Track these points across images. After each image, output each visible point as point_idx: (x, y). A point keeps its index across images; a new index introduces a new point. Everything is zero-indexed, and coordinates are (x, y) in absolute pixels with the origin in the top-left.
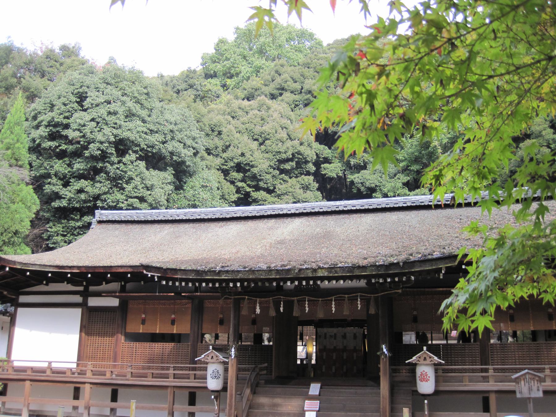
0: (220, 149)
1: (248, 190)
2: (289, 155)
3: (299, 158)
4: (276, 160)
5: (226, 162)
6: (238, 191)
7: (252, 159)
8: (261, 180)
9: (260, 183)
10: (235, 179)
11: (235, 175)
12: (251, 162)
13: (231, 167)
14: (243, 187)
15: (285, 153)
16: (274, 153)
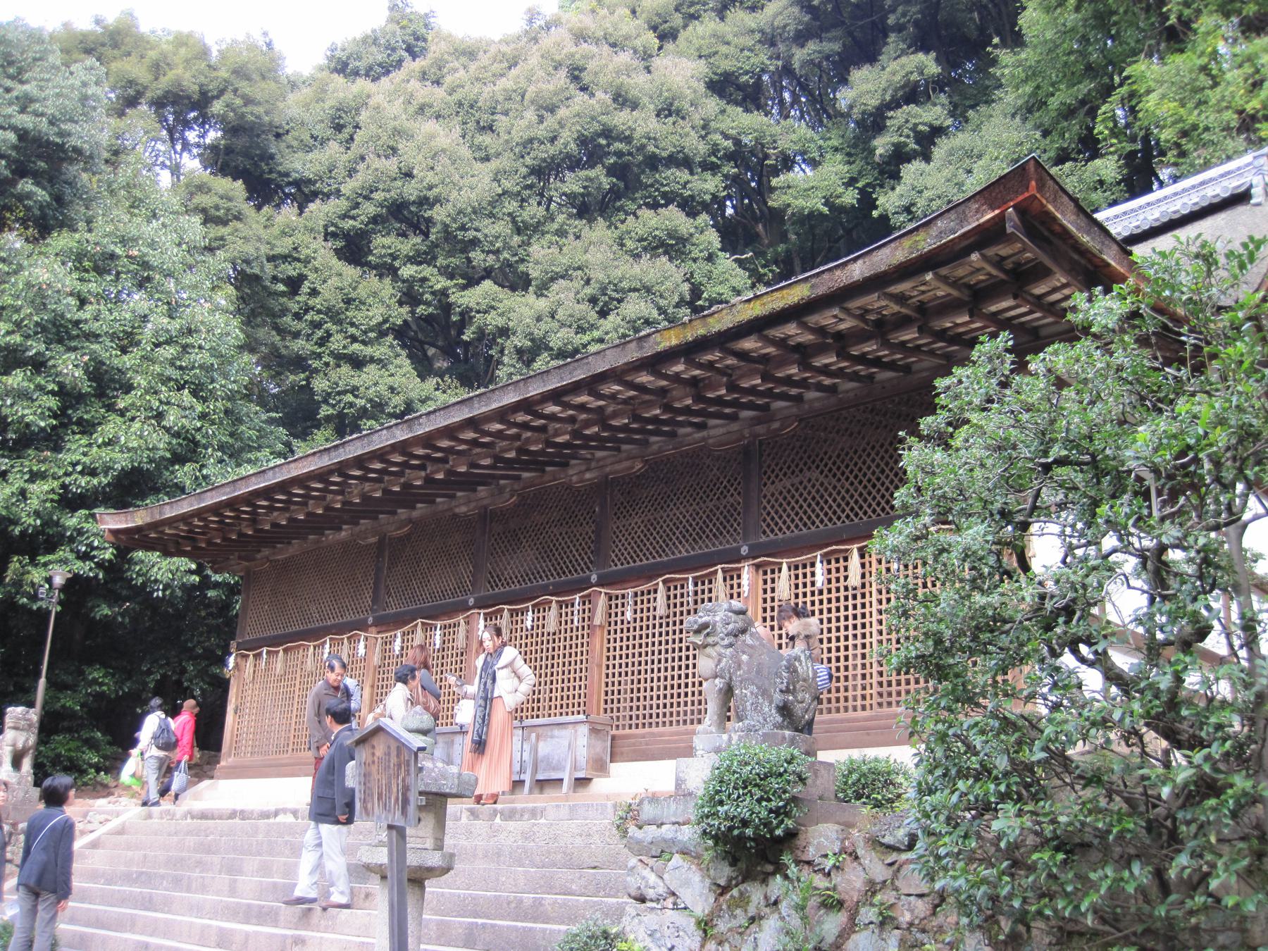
0: (340, 172)
1: (441, 283)
2: (567, 141)
3: (619, 154)
4: (524, 170)
5: (357, 206)
6: (410, 297)
7: (430, 178)
8: (474, 243)
9: (472, 255)
10: (394, 257)
11: (384, 243)
12: (430, 188)
13: (374, 220)
14: (424, 280)
15: (553, 140)
16: (517, 150)
